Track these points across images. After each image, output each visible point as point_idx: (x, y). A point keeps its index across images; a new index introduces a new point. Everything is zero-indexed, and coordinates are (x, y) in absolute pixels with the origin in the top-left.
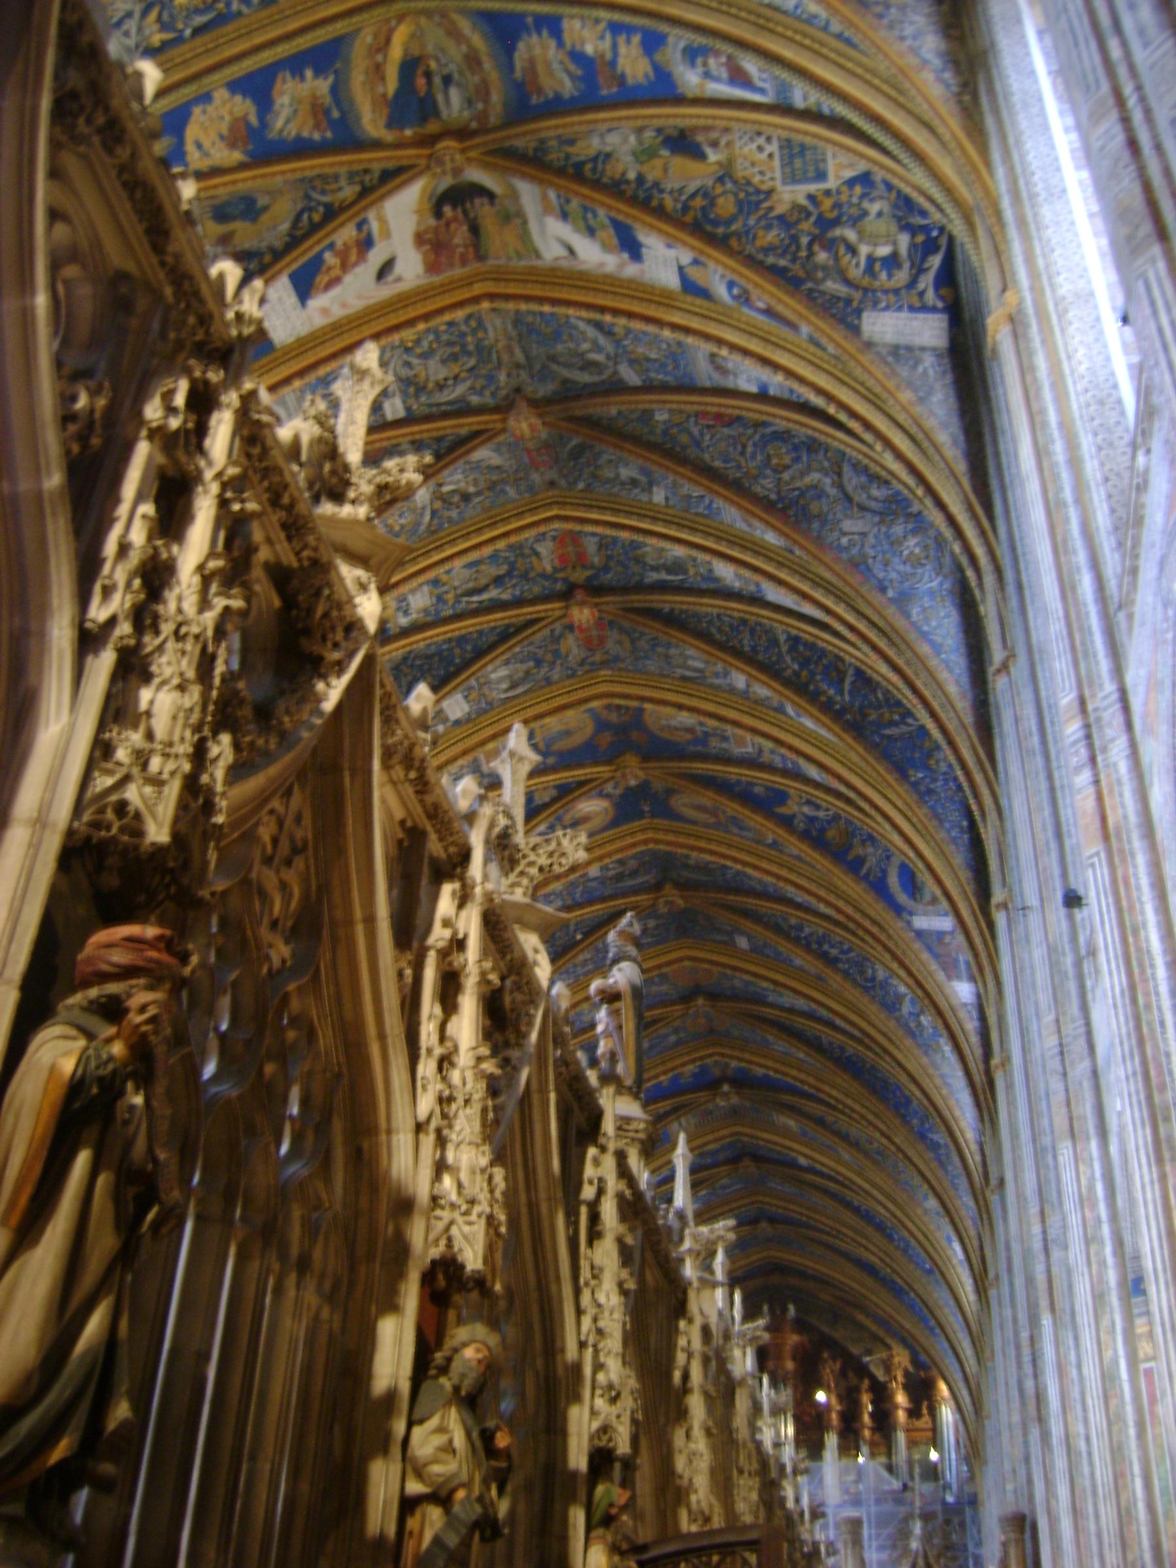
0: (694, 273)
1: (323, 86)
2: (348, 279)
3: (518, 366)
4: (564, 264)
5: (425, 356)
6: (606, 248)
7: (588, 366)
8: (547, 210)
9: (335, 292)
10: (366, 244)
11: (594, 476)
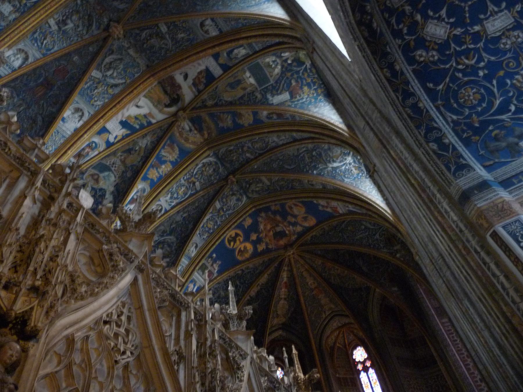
0: (105, 136)
1: (221, 125)
2: (196, 74)
3: (129, 48)
4: (137, 100)
5: (161, 48)
6: (129, 117)
7: (109, 66)
8: (150, 114)
9: (199, 70)
10: (194, 84)
11: (78, 12)
